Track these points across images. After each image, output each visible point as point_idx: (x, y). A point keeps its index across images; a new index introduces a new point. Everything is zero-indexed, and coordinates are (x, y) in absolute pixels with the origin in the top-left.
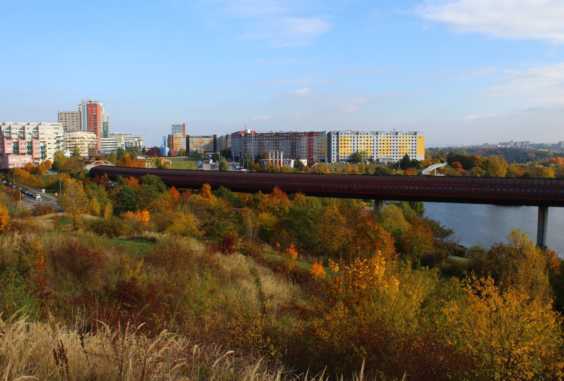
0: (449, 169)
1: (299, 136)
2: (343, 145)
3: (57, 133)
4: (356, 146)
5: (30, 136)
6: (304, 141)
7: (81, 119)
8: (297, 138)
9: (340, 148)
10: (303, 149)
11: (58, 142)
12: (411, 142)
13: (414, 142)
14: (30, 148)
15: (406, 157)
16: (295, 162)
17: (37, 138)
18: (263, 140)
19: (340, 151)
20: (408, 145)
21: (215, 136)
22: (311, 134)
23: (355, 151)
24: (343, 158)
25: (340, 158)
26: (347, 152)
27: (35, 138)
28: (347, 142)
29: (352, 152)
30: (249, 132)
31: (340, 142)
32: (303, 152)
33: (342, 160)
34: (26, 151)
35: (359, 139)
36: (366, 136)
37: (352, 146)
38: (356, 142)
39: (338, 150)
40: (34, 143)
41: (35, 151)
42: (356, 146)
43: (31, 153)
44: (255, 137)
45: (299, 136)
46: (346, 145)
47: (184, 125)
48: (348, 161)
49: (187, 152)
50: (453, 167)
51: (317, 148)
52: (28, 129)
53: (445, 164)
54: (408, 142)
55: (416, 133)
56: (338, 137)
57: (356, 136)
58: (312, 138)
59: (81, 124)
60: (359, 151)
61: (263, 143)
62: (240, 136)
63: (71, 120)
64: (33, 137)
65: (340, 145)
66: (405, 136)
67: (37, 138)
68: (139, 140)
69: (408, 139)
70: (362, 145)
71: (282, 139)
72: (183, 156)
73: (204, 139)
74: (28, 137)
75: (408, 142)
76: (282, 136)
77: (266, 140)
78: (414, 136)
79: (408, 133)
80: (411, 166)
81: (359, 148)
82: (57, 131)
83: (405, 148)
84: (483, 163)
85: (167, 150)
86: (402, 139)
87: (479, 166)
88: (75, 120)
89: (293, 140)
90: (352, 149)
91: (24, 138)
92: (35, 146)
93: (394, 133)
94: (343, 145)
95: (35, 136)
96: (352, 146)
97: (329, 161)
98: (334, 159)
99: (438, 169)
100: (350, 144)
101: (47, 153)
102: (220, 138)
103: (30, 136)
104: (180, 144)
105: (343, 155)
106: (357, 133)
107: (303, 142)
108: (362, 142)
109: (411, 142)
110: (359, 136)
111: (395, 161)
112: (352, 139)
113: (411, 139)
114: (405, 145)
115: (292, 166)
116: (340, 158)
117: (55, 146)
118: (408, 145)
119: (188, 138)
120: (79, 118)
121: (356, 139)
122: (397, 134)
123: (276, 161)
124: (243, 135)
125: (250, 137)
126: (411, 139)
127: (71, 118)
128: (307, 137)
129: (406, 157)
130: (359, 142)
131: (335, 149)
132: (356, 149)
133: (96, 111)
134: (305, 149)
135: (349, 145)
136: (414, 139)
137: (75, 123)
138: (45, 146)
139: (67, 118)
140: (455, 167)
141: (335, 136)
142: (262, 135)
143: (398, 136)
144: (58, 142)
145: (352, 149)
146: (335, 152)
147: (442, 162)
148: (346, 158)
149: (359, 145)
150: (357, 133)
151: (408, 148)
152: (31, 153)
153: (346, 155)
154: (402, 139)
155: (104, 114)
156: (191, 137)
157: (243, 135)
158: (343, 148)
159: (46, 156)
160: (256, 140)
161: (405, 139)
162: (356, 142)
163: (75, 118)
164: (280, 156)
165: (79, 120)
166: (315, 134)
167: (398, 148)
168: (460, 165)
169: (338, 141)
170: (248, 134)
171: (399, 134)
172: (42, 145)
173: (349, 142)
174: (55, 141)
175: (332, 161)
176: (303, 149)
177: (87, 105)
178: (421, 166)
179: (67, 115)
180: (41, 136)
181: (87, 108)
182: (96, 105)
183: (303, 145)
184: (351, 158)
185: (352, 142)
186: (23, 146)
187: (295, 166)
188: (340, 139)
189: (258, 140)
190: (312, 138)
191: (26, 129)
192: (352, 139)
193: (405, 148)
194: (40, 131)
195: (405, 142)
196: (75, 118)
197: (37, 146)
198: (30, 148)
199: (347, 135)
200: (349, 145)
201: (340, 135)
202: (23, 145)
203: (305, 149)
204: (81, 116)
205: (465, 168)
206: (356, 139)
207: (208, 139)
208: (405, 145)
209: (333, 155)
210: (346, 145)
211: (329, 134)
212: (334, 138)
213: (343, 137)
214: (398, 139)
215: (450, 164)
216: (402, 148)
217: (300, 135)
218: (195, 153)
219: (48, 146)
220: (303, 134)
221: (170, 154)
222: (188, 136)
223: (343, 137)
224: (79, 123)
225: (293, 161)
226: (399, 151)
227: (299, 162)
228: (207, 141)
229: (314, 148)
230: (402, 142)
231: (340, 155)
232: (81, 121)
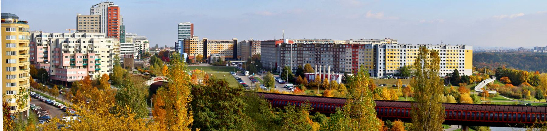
0: (499, 84)
1: (343, 48)
2: (390, 59)
3: (109, 47)
4: (403, 59)
5: (85, 49)
6: (349, 52)
7: (100, 23)
8: (341, 50)
9: (387, 62)
10: (346, 61)
11: (111, 55)
12: (459, 56)
13: (462, 56)
14: (86, 61)
15: (456, 72)
16: (343, 77)
17: (92, 51)
18: (303, 51)
19: (387, 65)
20: (456, 59)
21: (235, 41)
22: (356, 46)
23: (403, 65)
24: (390, 72)
25: (387, 72)
26: (393, 66)
27: (89, 51)
28: (394, 55)
29: (400, 66)
30: (287, 41)
31: (387, 55)
32: (346, 65)
33: (389, 74)
34: (81, 64)
35: (407, 52)
36: (414, 49)
37: (400, 59)
38: (403, 56)
39: (384, 64)
40: (89, 56)
41: (90, 64)
42: (403, 59)
43: (86, 66)
44: (294, 47)
45: (343, 48)
46: (393, 59)
47: (192, 25)
49: (205, 59)
50: (502, 83)
51: (362, 62)
52: (84, 42)
54: (456, 56)
55: (463, 47)
56: (385, 50)
57: (403, 50)
58: (357, 50)
59: (100, 28)
60: (407, 65)
61: (302, 54)
62: (277, 46)
63: (90, 24)
64: (87, 50)
65: (387, 59)
66: (453, 49)
67: (92, 51)
68: (145, 42)
69: (456, 53)
70: (410, 59)
71: (324, 51)
72: (204, 62)
73: (223, 44)
74: (84, 51)
75: (456, 56)
76: (324, 48)
77: (306, 51)
78: (462, 50)
79: (456, 47)
80: (461, 81)
81: (406, 62)
82: (109, 44)
83: (453, 62)
84: (531, 79)
85: (186, 55)
86: (449, 52)
87: (528, 82)
88: (94, 24)
89: (336, 51)
90: (400, 62)
91: (80, 52)
92: (90, 59)
93: (442, 46)
94: (390, 59)
95: (90, 49)
96: (400, 59)
97: (376, 75)
98: (380, 74)
99: (488, 85)
100: (398, 57)
101: (100, 66)
102: (241, 43)
103: (85, 49)
104: (197, 50)
105: (390, 69)
106: (405, 46)
107: (347, 54)
108: (410, 56)
109: (459, 56)
110: (407, 49)
111: (443, 75)
112: (400, 52)
113: (459, 53)
114: (453, 59)
115: (340, 81)
116: (387, 72)
117: (108, 59)
118: (456, 59)
119: (205, 42)
120: (98, 22)
121: (403, 52)
122: (445, 47)
123: (322, 76)
124: (280, 44)
125: (288, 47)
126: (459, 53)
127: (90, 22)
128: (351, 49)
129: (456, 72)
130: (407, 55)
131: (382, 62)
132: (403, 62)
133: (117, 14)
134: (349, 61)
135: (396, 59)
136: (462, 53)
137: (94, 27)
138: (99, 59)
139: (87, 22)
140: (505, 83)
141: (382, 49)
142: (301, 45)
143: (446, 50)
144: (111, 55)
145: (400, 62)
146: (382, 66)
147: (491, 77)
148: (393, 72)
149: (406, 59)
151: (456, 62)
152: (86, 66)
153: (393, 69)
154: (449, 52)
155: (125, 17)
156: (209, 42)
157: (280, 44)
158: (390, 62)
159: (99, 69)
160: (294, 50)
161: (453, 53)
162: (403, 56)
163: (94, 22)
164: (323, 68)
165: (98, 24)
166: (360, 47)
167: (446, 62)
168: (509, 81)
169: (384, 54)
170: (287, 44)
171: (447, 47)
172: (96, 58)
173: (396, 55)
174: (108, 54)
175: (379, 75)
176: (346, 61)
177: (108, 8)
178: (471, 81)
179: (87, 19)
180: (95, 49)
181: (107, 12)
182: (116, 9)
183: (347, 58)
184: (398, 72)
185: (400, 55)
186: (79, 60)
187: (343, 81)
188: (387, 52)
189: (297, 51)
190: (357, 50)
191: (82, 42)
192: (400, 52)
193: (453, 62)
194: (95, 44)
195: (453, 56)
196: (94, 22)
197: (92, 58)
198: (86, 61)
199: (394, 48)
200: (396, 59)
201: (387, 48)
202: (79, 58)
203: (349, 61)
204: (100, 21)
205: (514, 84)
206: (403, 52)
207: (227, 44)
208: (453, 59)
209: (379, 69)
210: (393, 59)
211: (376, 46)
212: (381, 51)
213: (390, 51)
214: (446, 53)
215: (498, 79)
216: (449, 62)
217: (344, 46)
218: (219, 60)
219: (102, 59)
220: (347, 46)
221: (188, 60)
222: (206, 40)
223: (390, 51)
224: (98, 27)
225: (341, 76)
226: (446, 66)
227: (346, 76)
228: (226, 46)
229: (359, 62)
230: (449, 56)
231: (387, 69)
232: (100, 26)
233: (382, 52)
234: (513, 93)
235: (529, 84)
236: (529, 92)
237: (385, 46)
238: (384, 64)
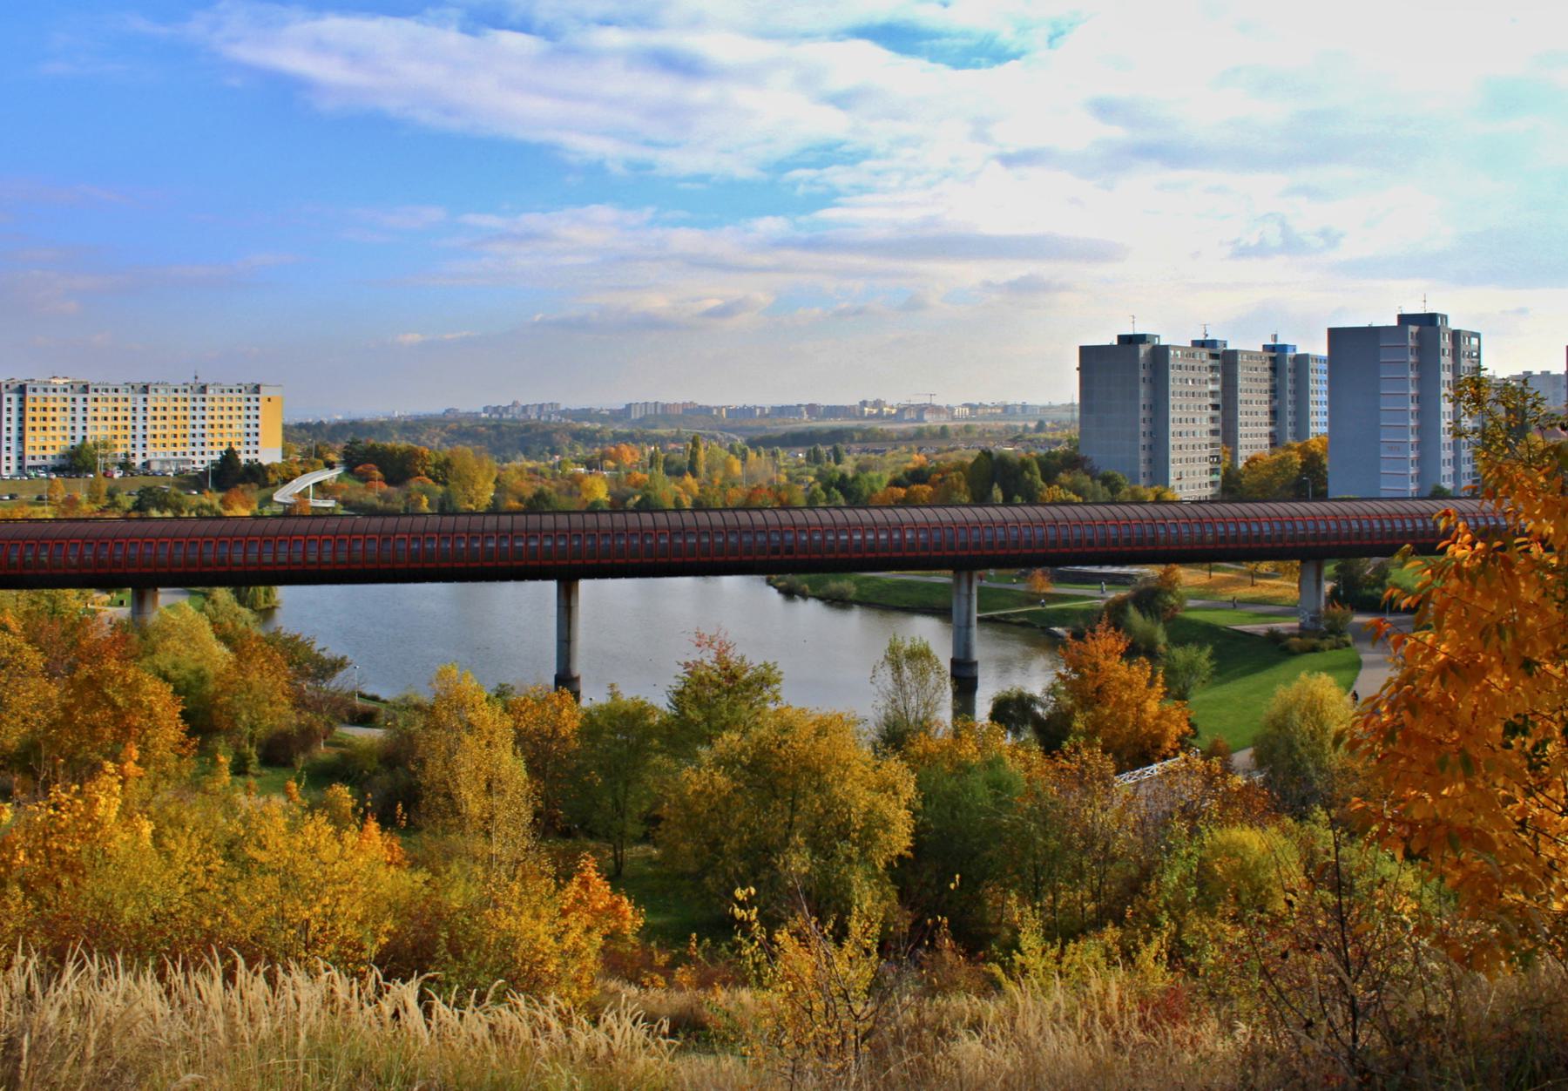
0: (350, 483)
4: (79, 424)
38: (79, 414)
39: (21, 439)
42: (79, 424)
48: (55, 470)
53: (338, 471)
84: (436, 466)
87: (428, 474)
99: (318, 485)
121: (80, 405)
132: (79, 433)
140: (365, 478)
147: (330, 465)
150: (86, 389)
162: (79, 414)
168: (378, 474)
178: (273, 478)
205: (390, 481)
206: (80, 405)
233: (15, 405)
234: (380, 504)
235: (431, 482)
236: (425, 499)
237: (22, 389)
238: (21, 439)
